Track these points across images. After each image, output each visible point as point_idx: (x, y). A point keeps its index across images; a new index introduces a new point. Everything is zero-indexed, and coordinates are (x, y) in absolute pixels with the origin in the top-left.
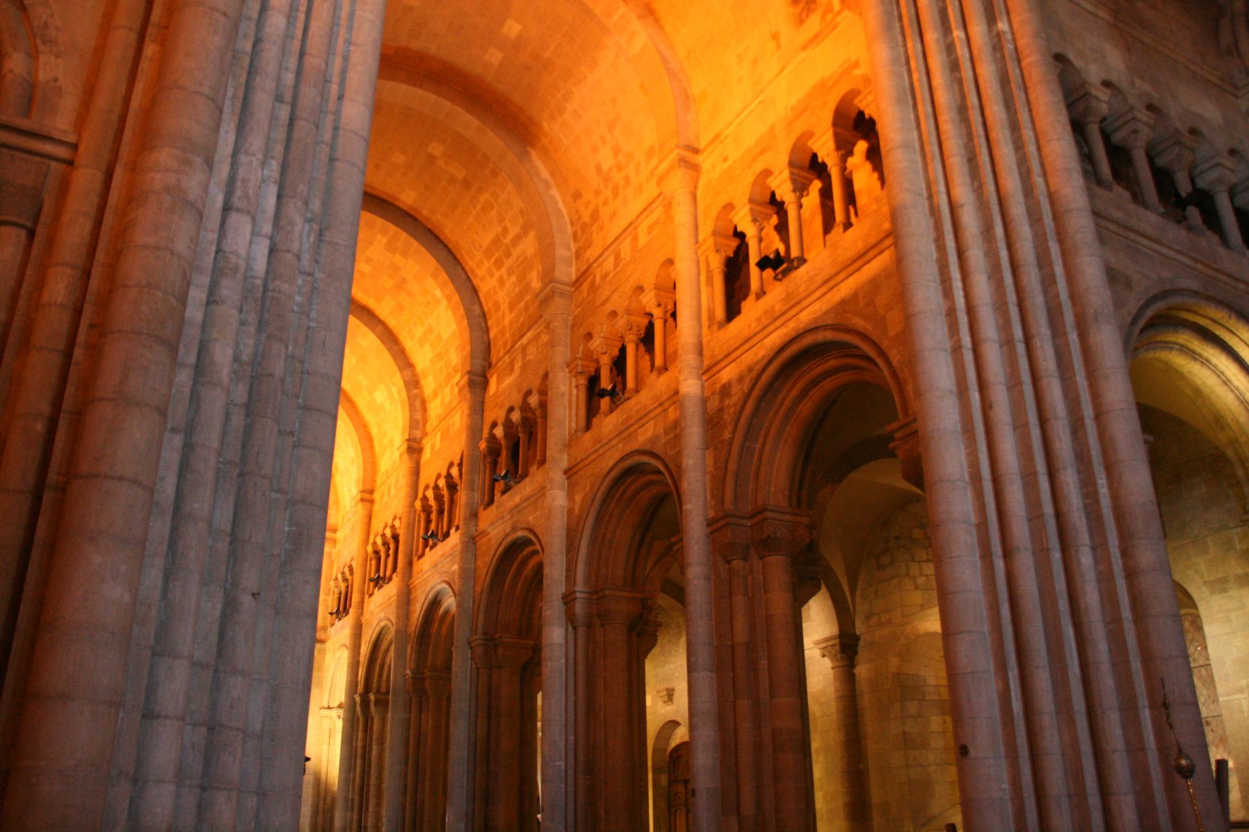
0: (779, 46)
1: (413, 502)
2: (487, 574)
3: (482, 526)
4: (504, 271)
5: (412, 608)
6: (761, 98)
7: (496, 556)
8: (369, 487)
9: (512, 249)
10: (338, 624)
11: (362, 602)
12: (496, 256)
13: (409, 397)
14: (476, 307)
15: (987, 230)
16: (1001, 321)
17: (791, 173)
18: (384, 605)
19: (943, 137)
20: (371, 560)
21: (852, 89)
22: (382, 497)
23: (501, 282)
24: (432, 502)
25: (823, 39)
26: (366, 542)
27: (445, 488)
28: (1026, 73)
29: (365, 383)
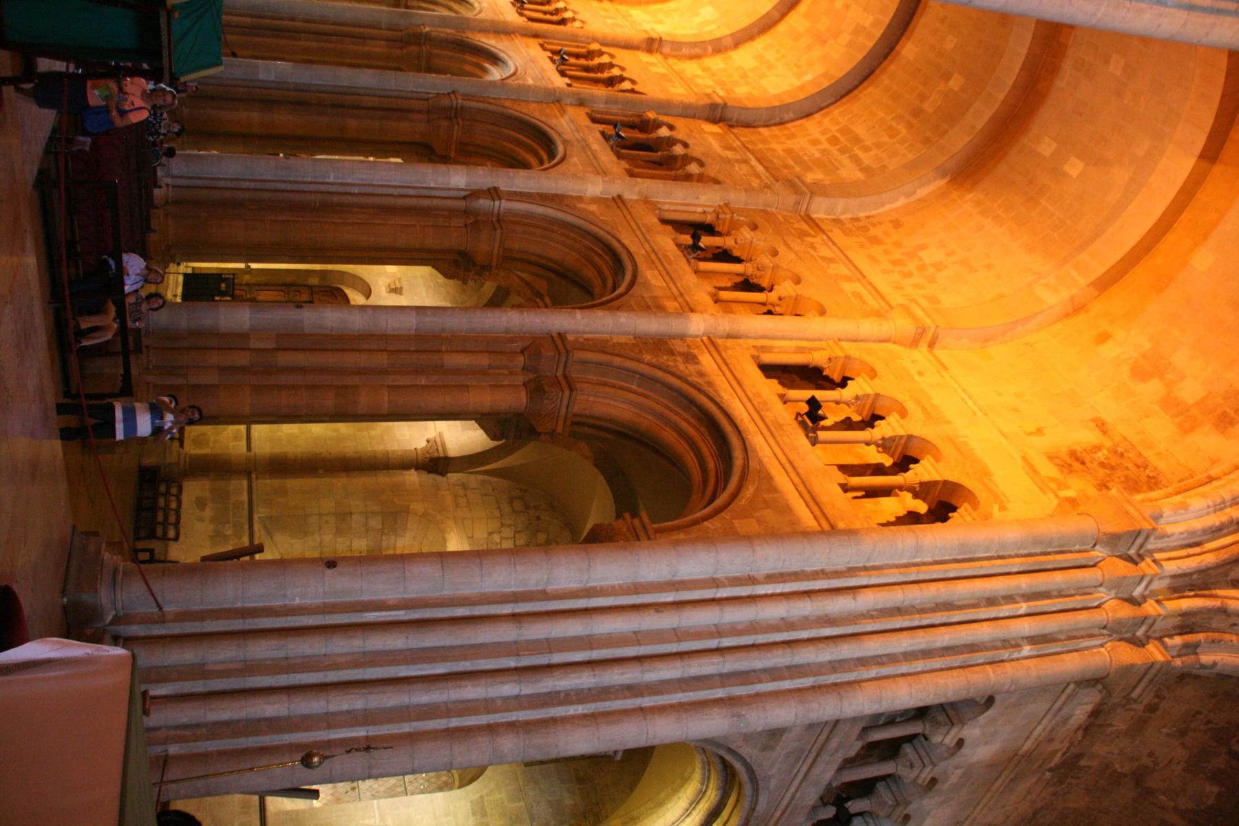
2: (523, 113)
3: (571, 111)
4: (825, 145)
5: (491, 36)
6: (979, 413)
9: (847, 155)
12: (842, 139)
14: (791, 115)
15: (829, 621)
16: (740, 627)
17: (901, 437)
18: (495, 8)
19: (923, 585)
21: (979, 502)
23: (815, 142)
24: (597, 61)
25: (1032, 479)
27: (609, 75)
28: (977, 668)
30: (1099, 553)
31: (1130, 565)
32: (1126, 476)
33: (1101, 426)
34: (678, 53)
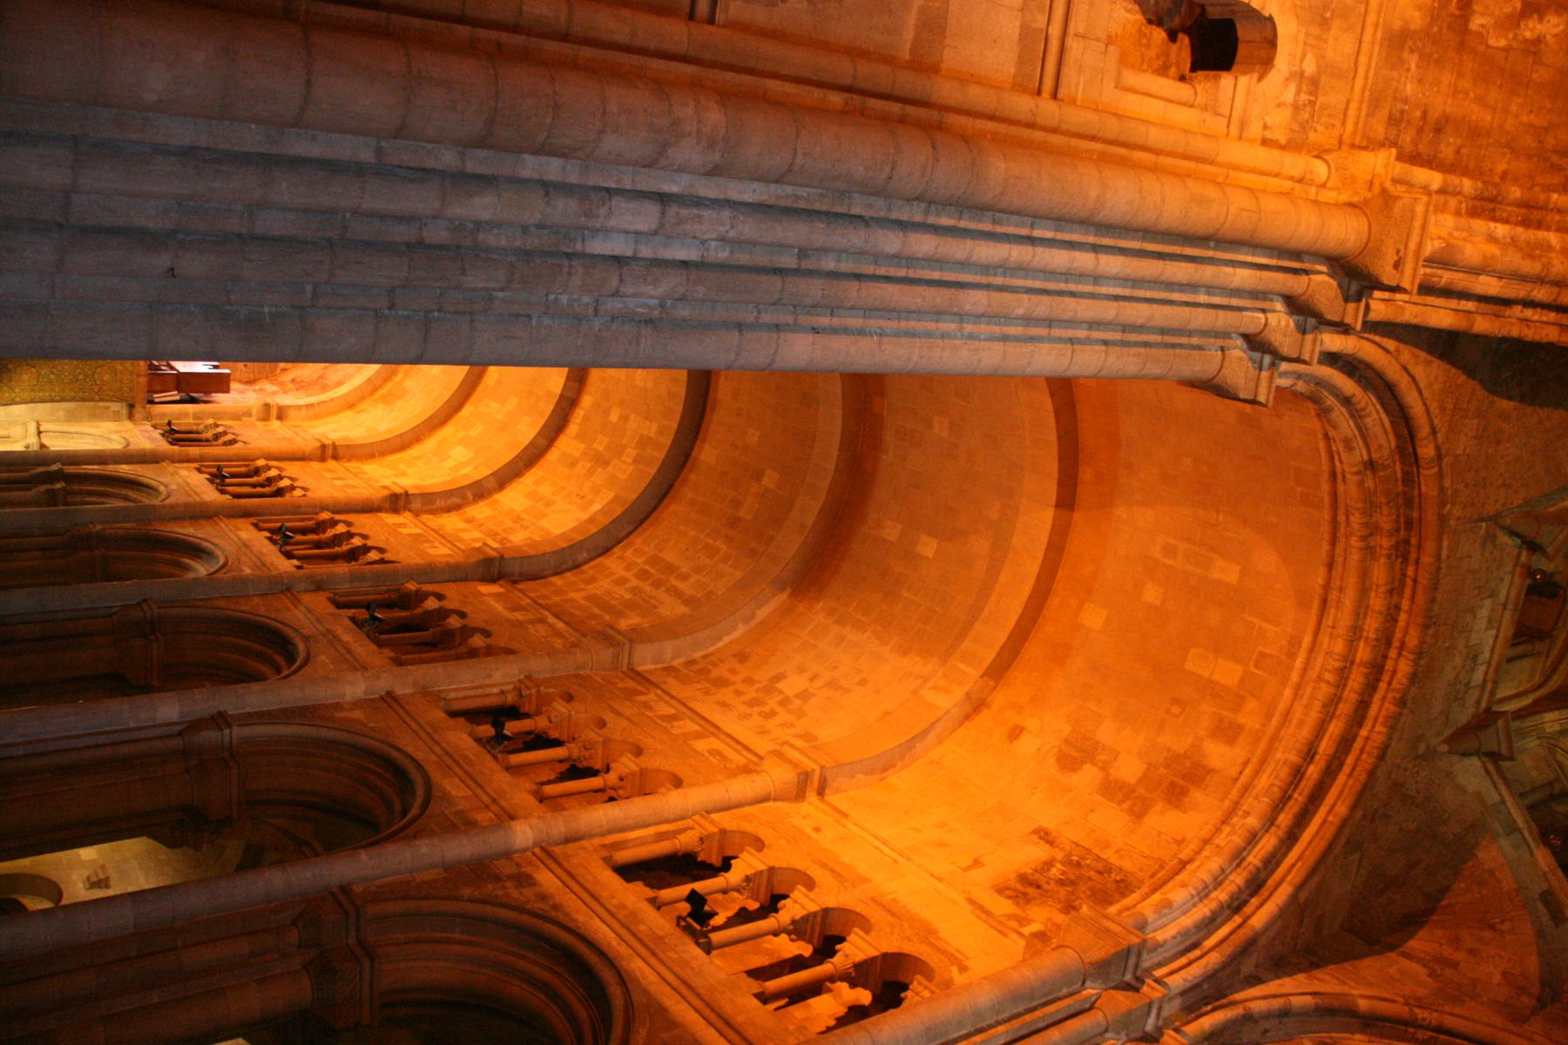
0: (968, 868)
1: (327, 510)
2: (242, 612)
6: (901, 860)
7: (268, 621)
8: (341, 452)
10: (157, 434)
11: (189, 460)
13: (462, 487)
17: (815, 914)
18: (187, 488)
20: (247, 466)
21: (932, 970)
22: (330, 471)
24: (330, 533)
25: (986, 922)
26: (269, 457)
27: (350, 546)
29: (473, 433)
30: (1091, 991)
31: (1131, 994)
32: (1091, 889)
33: (1045, 836)
34: (432, 507)
